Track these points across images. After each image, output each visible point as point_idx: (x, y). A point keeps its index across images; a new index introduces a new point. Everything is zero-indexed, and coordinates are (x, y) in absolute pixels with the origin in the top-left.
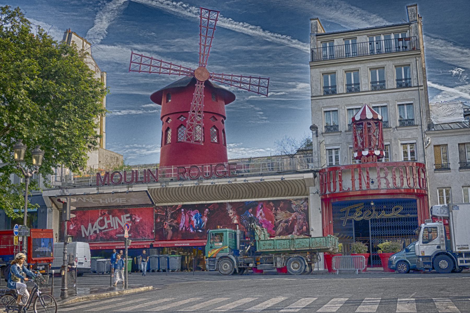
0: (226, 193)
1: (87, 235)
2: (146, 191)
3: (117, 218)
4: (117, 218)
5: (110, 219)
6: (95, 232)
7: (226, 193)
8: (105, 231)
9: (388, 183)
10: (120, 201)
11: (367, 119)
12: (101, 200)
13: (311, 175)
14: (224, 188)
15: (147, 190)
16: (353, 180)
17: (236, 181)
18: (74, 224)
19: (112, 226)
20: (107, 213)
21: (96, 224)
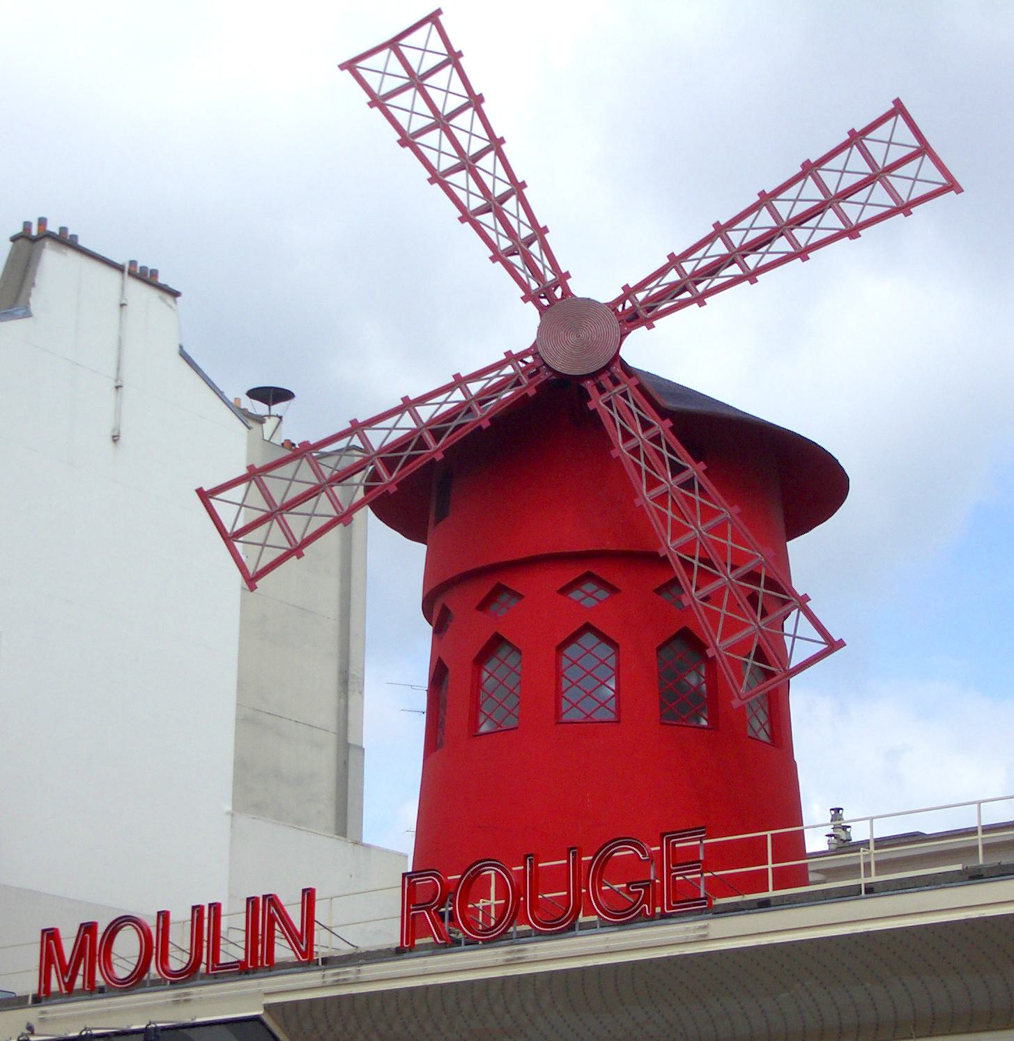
2: (256, 1019)
15: (260, 1012)
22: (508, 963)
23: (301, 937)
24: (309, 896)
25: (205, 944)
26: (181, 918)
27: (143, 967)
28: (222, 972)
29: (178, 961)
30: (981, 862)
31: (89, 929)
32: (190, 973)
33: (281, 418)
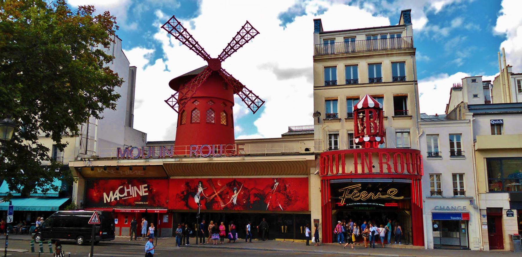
1: (109, 201)
2: (162, 165)
3: (135, 188)
5: (129, 189)
6: (116, 199)
8: (125, 198)
10: (139, 173)
11: (369, 108)
12: (121, 172)
13: (313, 157)
14: (232, 165)
15: (162, 164)
17: (244, 160)
18: (97, 191)
19: (131, 194)
20: (127, 183)
21: (117, 192)
22: (210, 160)
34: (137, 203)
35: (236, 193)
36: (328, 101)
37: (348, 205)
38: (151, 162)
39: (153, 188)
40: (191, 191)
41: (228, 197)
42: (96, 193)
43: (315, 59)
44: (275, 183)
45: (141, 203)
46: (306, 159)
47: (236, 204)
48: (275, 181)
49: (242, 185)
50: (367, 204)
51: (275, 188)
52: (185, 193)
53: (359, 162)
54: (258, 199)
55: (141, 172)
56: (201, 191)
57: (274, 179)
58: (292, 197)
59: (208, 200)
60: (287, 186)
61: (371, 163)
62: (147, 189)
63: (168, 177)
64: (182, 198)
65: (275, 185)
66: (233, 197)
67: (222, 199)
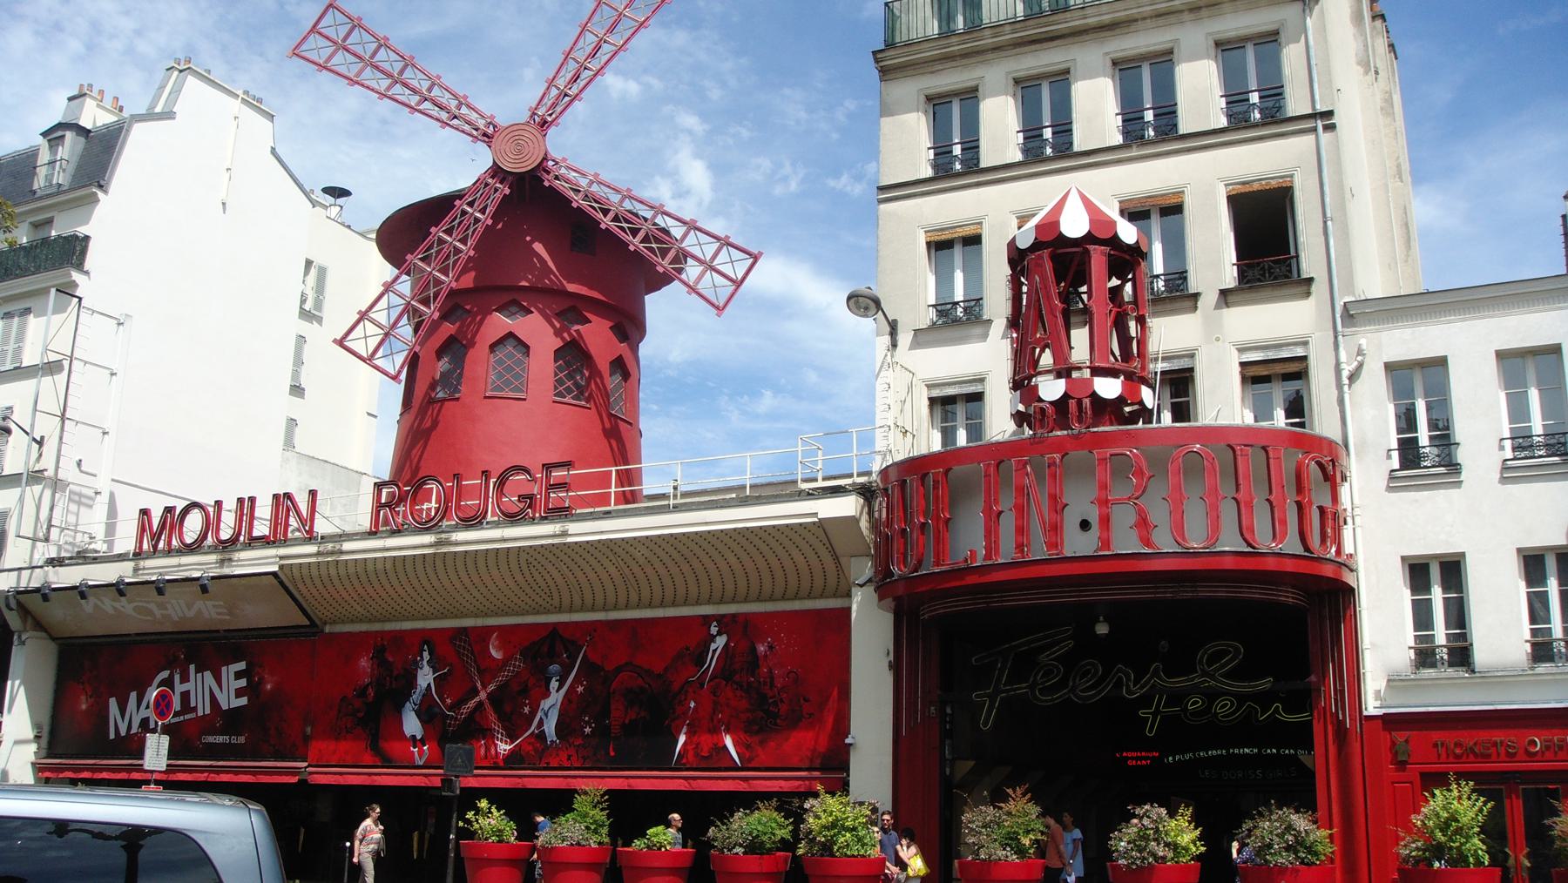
0: (539, 579)
2: (274, 574)
4: (208, 674)
7: (539, 579)
9: (1143, 525)
10: (209, 613)
14: (528, 563)
15: (275, 568)
16: (992, 518)
19: (193, 704)
20: (182, 656)
23: (306, 521)
24: (313, 493)
25: (244, 523)
26: (230, 505)
27: (203, 536)
28: (254, 542)
29: (225, 534)
30: (748, 493)
31: (169, 510)
32: (234, 540)
33: (342, 207)
34: (210, 739)
35: (558, 691)
36: (939, 246)
37: (1170, 759)
38: (239, 560)
39: (263, 678)
40: (391, 682)
41: (527, 710)
42: (87, 699)
43: (882, 64)
44: (712, 639)
45: (221, 739)
46: (815, 514)
47: (555, 739)
48: (714, 630)
49: (583, 652)
50: (1255, 751)
51: (712, 662)
52: (371, 693)
53: (1006, 502)
54: (643, 714)
55: (214, 606)
56: (429, 684)
57: (706, 620)
58: (781, 701)
59: (450, 725)
60: (762, 649)
61: (1057, 506)
62: (243, 683)
63: (313, 624)
64: (360, 715)
65: (713, 646)
66: (546, 709)
67: (503, 718)
